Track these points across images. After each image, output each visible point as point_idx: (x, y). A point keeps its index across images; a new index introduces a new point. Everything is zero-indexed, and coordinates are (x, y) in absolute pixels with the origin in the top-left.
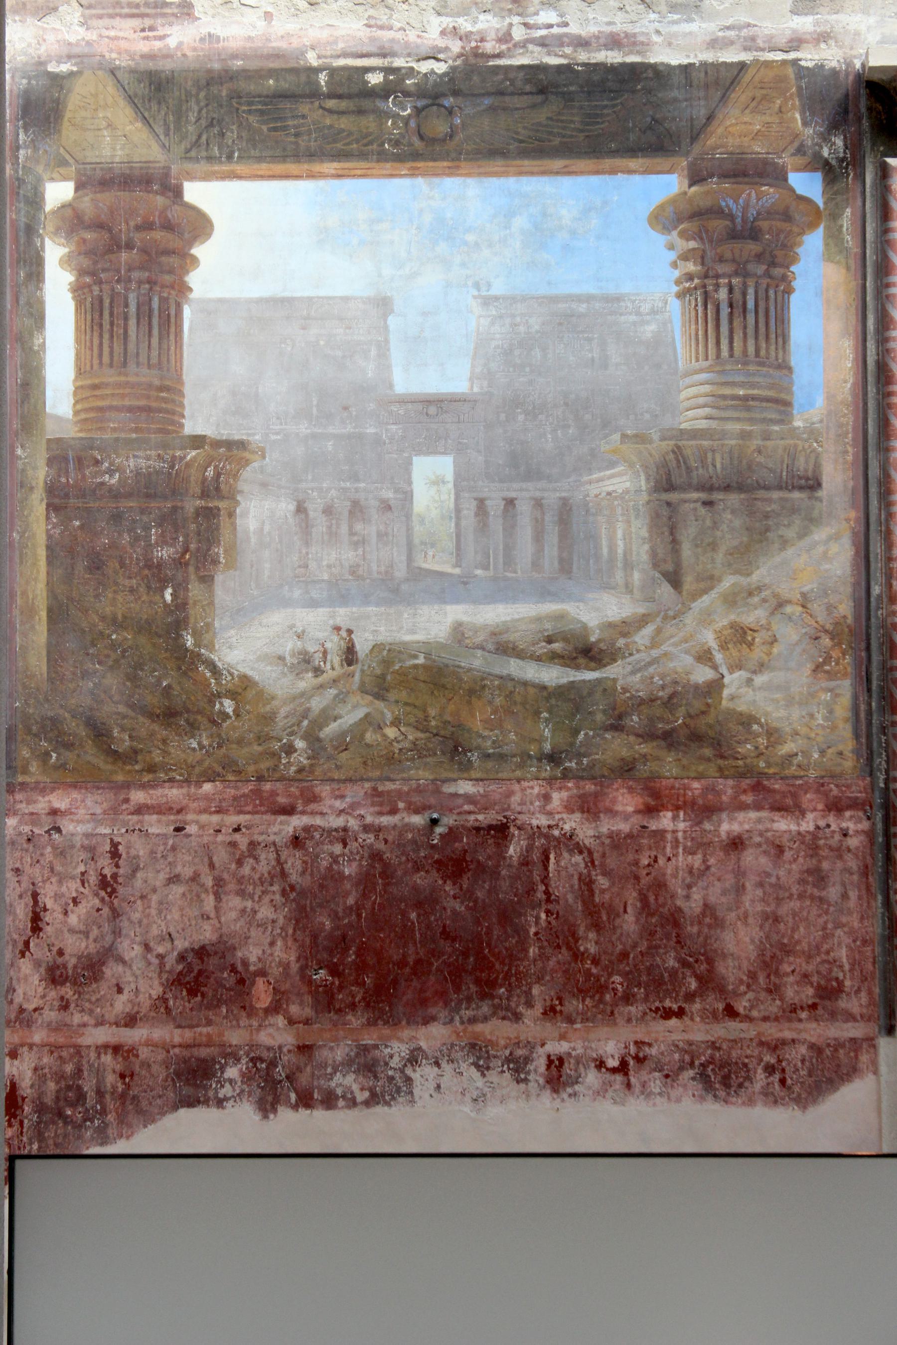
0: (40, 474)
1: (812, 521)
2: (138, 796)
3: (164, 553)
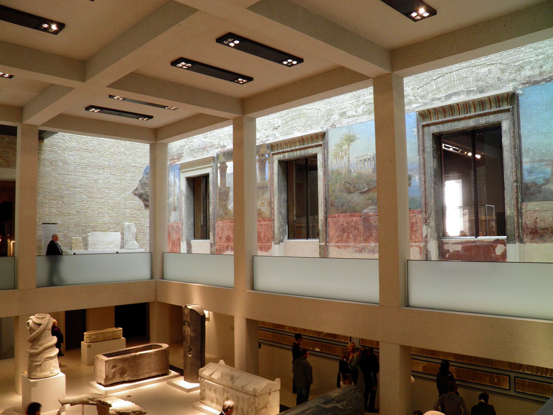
0: (218, 192)
2: (224, 222)
3: (225, 198)
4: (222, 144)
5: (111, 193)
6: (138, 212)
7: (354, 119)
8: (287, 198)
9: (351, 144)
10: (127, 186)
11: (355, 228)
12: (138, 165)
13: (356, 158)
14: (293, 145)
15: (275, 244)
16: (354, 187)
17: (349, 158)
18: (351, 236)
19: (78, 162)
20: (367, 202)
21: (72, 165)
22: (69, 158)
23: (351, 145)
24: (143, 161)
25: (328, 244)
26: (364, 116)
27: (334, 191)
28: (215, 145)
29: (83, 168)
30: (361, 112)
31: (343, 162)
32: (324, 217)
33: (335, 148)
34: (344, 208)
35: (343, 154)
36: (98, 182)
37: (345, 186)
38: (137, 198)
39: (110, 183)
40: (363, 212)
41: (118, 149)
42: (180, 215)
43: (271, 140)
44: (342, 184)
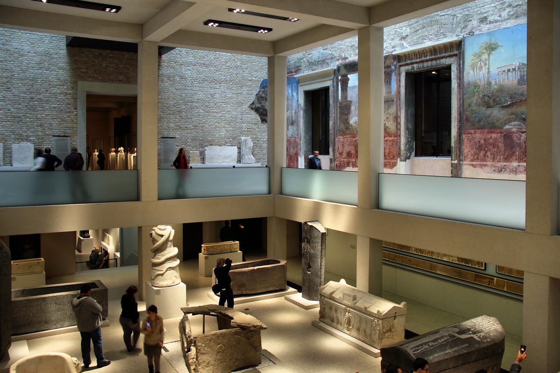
0: (339, 105)
1: (393, 105)
2: (345, 137)
4: (343, 56)
5: (228, 108)
6: (255, 127)
7: (496, 24)
8: (415, 113)
9: (492, 52)
10: (243, 101)
11: (493, 145)
12: (254, 79)
13: (497, 68)
14: (423, 55)
15: (401, 161)
16: (494, 100)
17: (489, 69)
18: (488, 154)
19: (195, 77)
20: (510, 117)
21: (189, 80)
22: (186, 73)
23: (492, 54)
24: (260, 74)
25: (461, 162)
26: (509, 21)
27: (470, 105)
28: (335, 57)
29: (199, 83)
30: (506, 16)
31: (481, 73)
32: (457, 133)
33: (473, 58)
34: (481, 124)
35: (483, 64)
36: (215, 96)
37: (483, 100)
38: (253, 112)
39: (226, 97)
40: (505, 128)
41: (234, 63)
42: (298, 130)
43: (398, 51)
44: (479, 98)
